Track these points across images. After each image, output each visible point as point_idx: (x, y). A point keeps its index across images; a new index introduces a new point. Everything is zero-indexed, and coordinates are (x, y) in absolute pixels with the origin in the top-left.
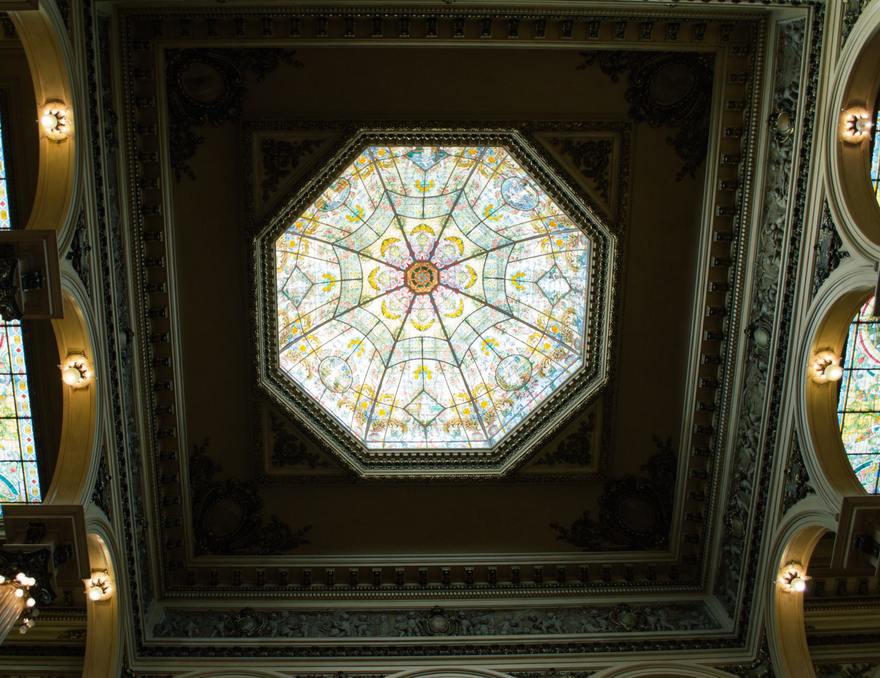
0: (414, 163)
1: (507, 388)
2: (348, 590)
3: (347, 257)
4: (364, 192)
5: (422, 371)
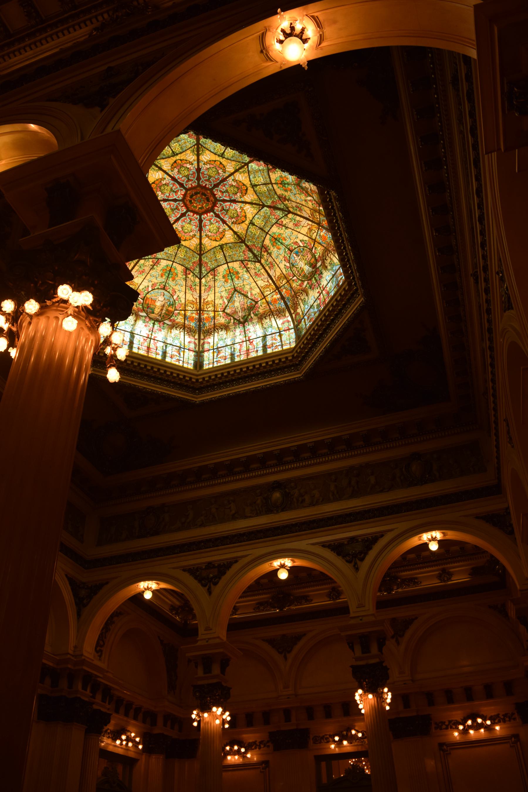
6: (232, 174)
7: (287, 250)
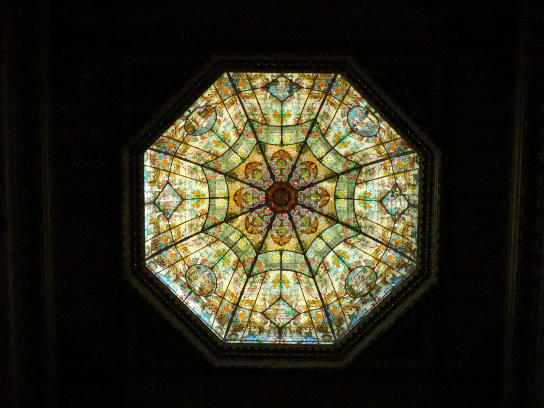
0: (271, 94)
1: (354, 295)
3: (215, 177)
4: (229, 120)
5: (281, 281)
6: (298, 237)
7: (213, 265)
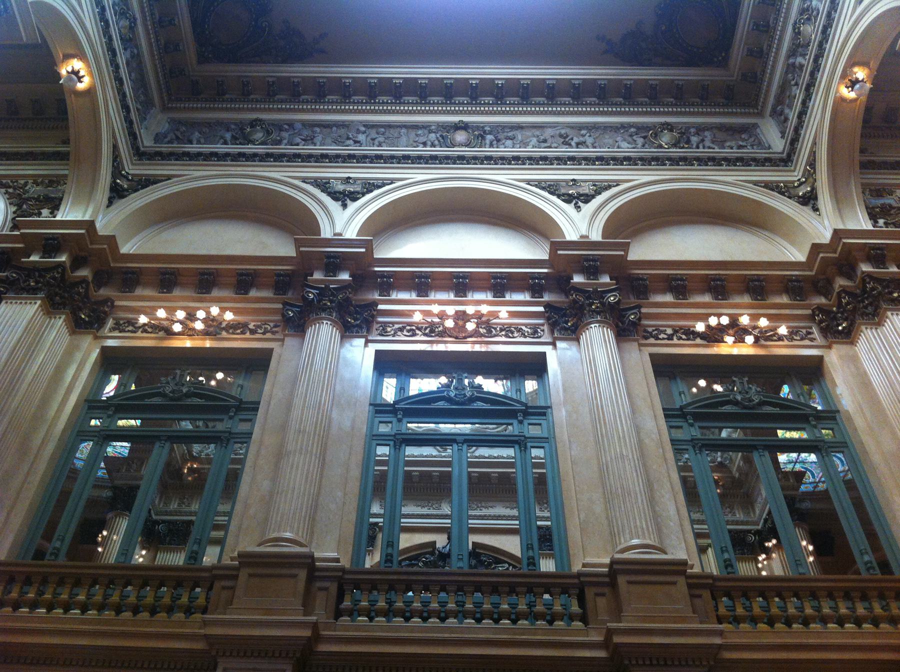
2: (366, 103)
